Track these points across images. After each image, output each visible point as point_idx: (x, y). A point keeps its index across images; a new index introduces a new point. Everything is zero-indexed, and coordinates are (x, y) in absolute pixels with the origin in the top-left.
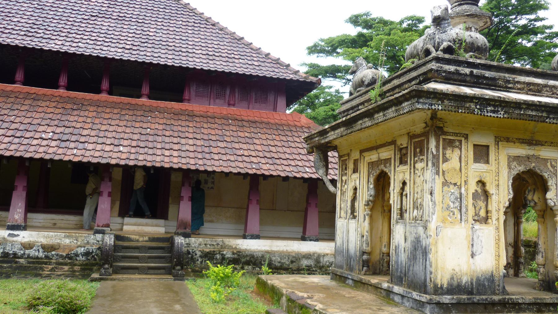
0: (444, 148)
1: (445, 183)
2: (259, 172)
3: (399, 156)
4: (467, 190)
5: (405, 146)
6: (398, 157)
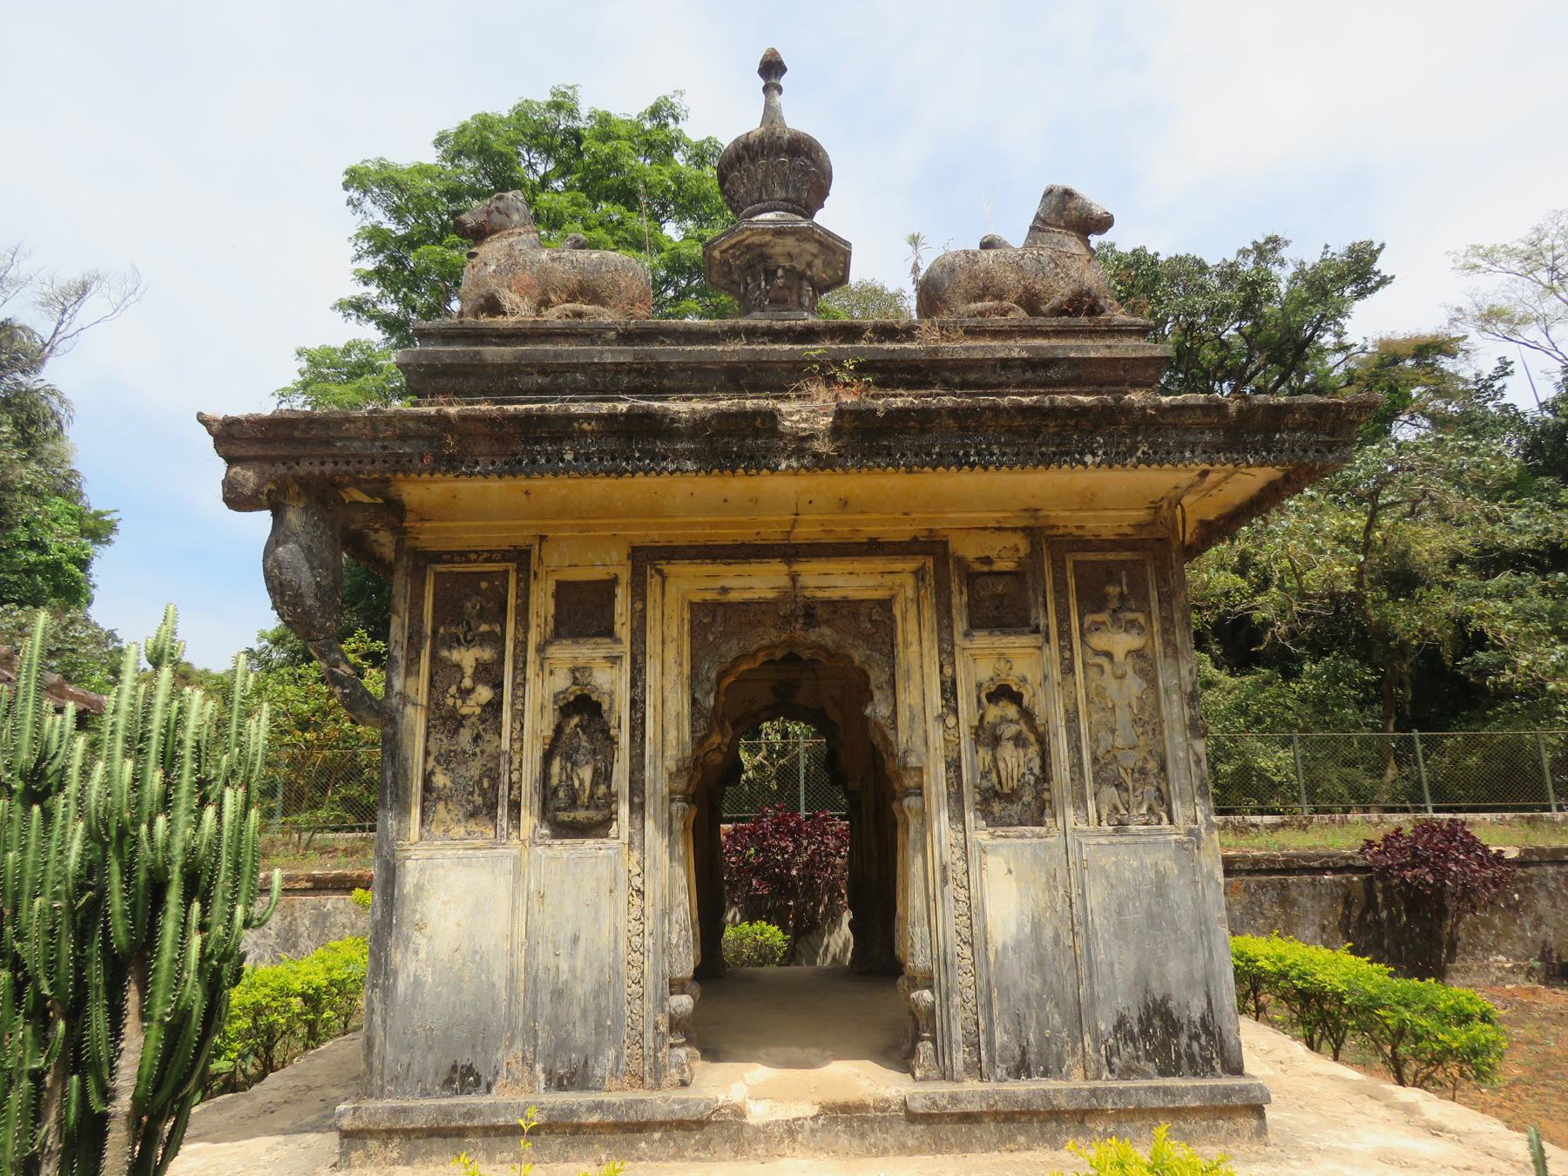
3: (965, 598)
5: (1007, 565)
6: (959, 600)
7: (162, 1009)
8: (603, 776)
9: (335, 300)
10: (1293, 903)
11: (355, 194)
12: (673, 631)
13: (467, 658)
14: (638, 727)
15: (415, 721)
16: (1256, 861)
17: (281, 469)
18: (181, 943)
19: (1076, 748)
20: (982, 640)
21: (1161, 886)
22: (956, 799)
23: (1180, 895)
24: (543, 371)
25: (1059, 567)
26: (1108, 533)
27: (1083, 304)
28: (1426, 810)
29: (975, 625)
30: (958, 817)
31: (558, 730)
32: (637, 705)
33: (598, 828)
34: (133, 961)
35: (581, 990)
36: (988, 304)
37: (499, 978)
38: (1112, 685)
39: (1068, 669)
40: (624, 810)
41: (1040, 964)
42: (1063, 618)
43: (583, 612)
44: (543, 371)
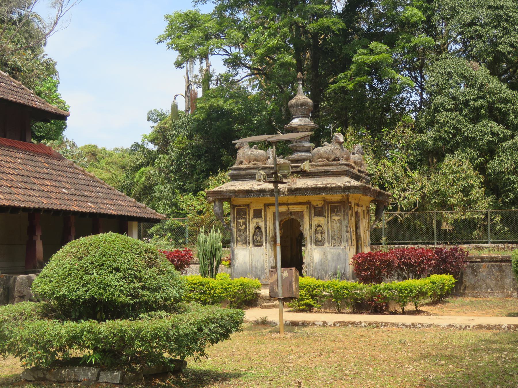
6: (313, 212)
7: (217, 259)
8: (261, 238)
10: (504, 271)
12: (271, 217)
13: (241, 221)
14: (266, 231)
15: (235, 230)
16: (492, 258)
17: (215, 197)
18: (218, 254)
19: (328, 234)
20: (316, 218)
21: (339, 254)
22: (311, 242)
23: (342, 256)
24: (250, 175)
25: (328, 206)
26: (336, 201)
27: (336, 159)
28: (433, 244)
29: (315, 215)
30: (311, 244)
31: (255, 231)
32: (265, 228)
33: (261, 246)
34: (214, 256)
35: (259, 267)
36: (321, 160)
37: (248, 265)
38: (335, 225)
39: (328, 222)
40: (264, 243)
41: (321, 265)
42: (328, 215)
43: (258, 214)
44: (250, 175)
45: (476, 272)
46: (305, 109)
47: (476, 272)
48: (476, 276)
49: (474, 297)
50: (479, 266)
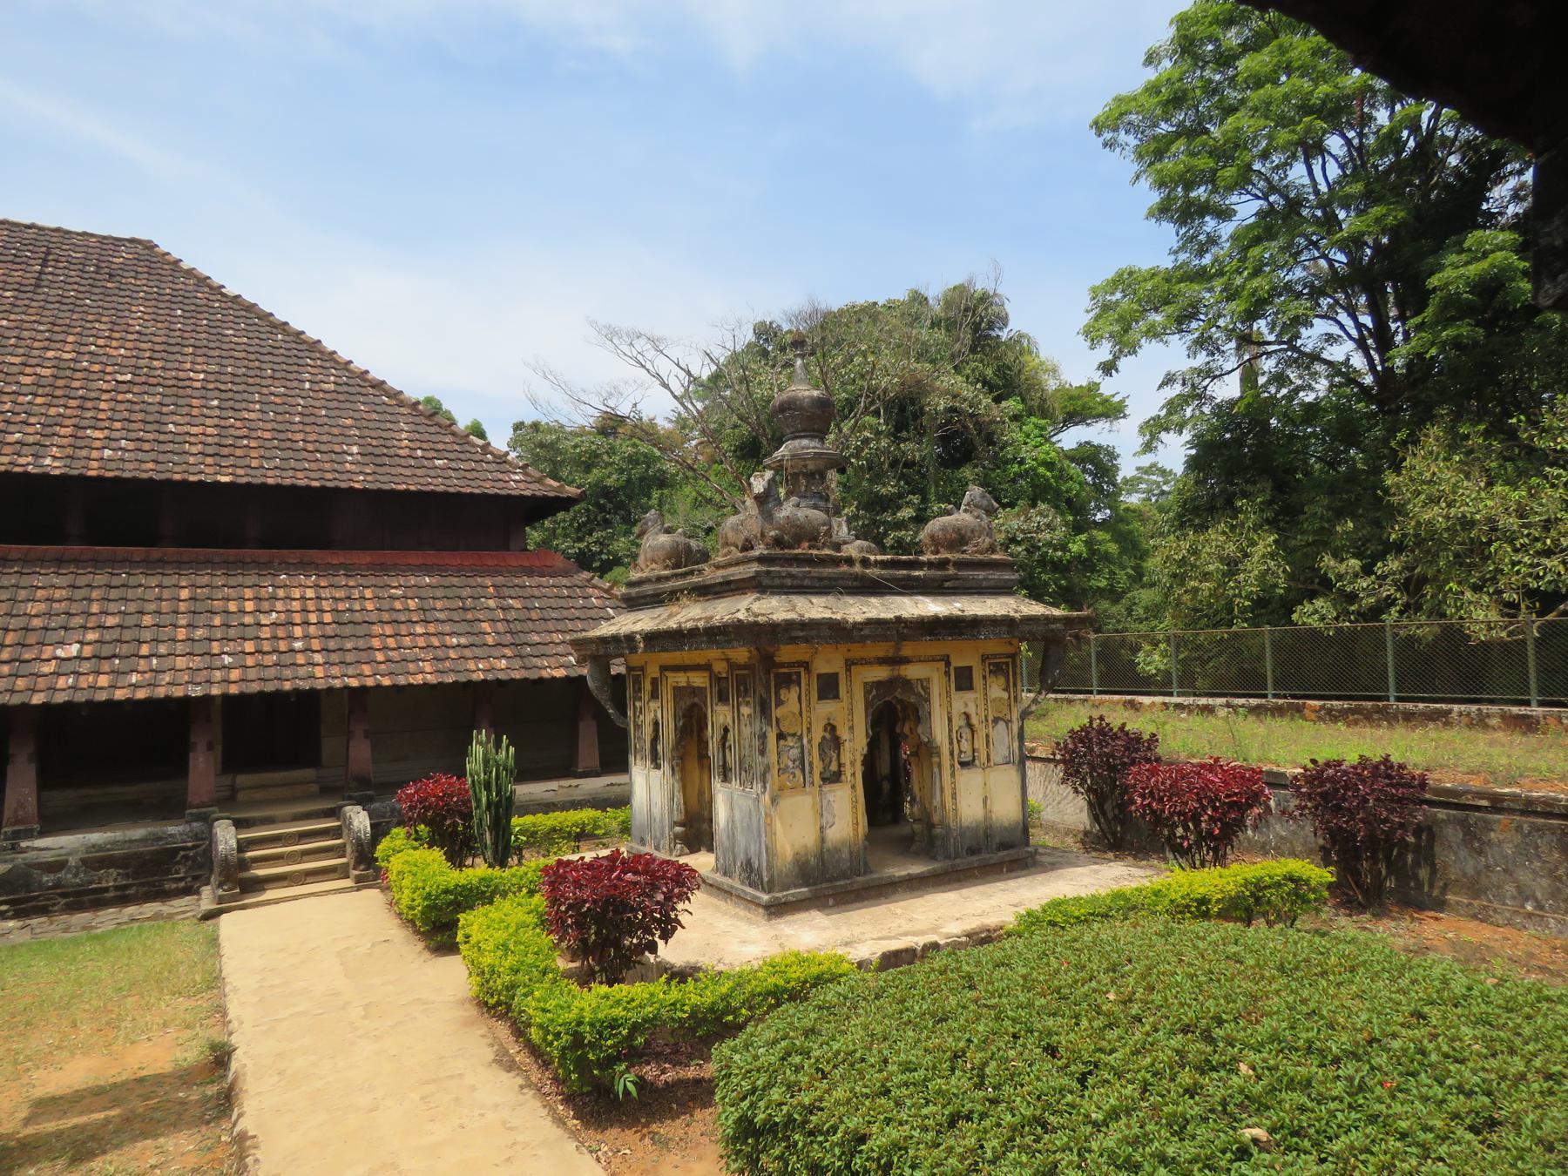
0: (778, 687)
1: (781, 736)
2: (490, 677)
4: (810, 741)
6: (715, 690)
9: (1145, 212)
11: (1108, 135)
13: (638, 704)
27: (747, 546)
45: (1479, 840)
46: (793, 417)
47: (1479, 840)
48: (1480, 852)
49: (1475, 917)
50: (1486, 821)
